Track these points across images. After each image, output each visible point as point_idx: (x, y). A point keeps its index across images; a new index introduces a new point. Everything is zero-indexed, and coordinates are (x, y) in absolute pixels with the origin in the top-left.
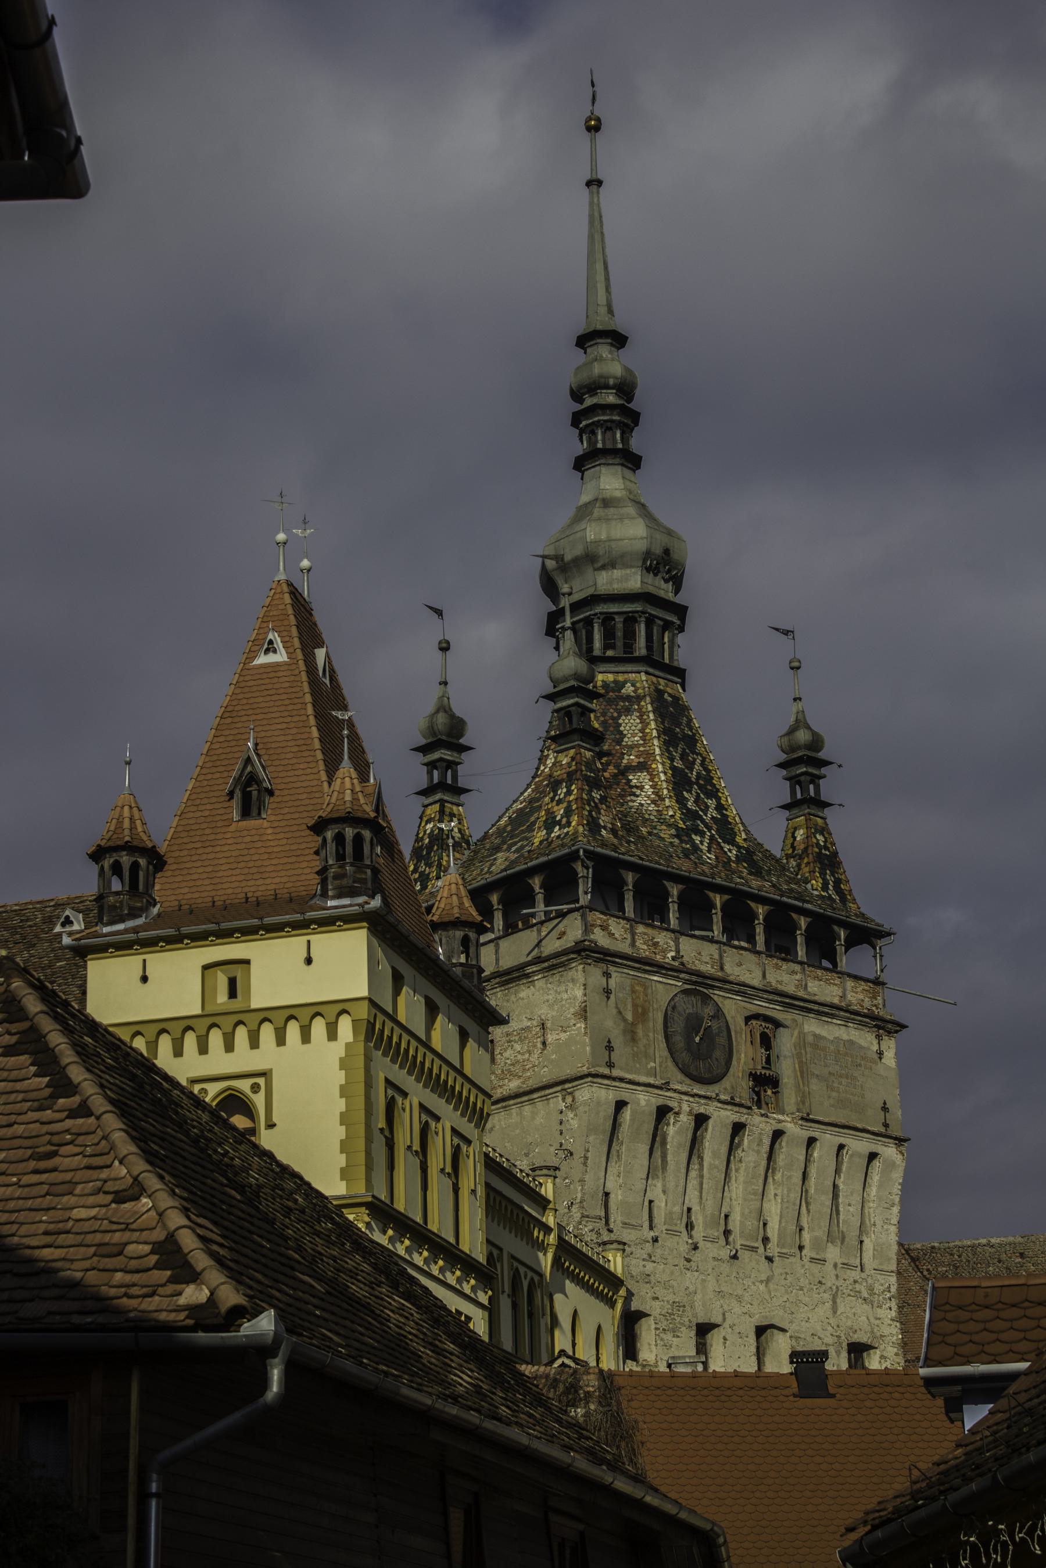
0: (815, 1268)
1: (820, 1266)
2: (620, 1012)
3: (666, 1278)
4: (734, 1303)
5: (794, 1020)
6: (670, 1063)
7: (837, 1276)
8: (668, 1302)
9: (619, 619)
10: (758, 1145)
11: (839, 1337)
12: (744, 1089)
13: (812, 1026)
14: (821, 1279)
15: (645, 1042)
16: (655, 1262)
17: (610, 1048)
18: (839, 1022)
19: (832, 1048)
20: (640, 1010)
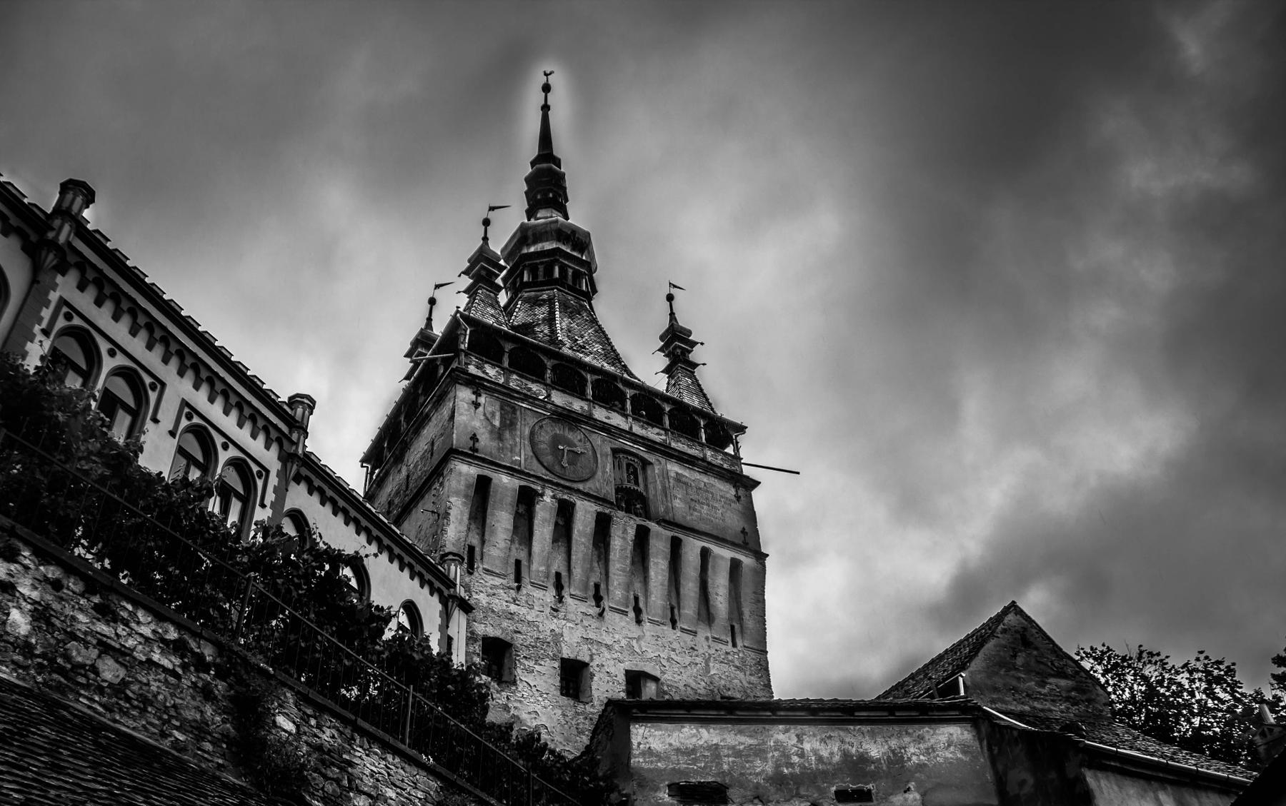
0: (688, 638)
1: (691, 636)
2: (488, 420)
3: (529, 618)
4: (603, 649)
5: (658, 460)
6: (535, 461)
7: (709, 647)
8: (531, 637)
9: (541, 268)
10: (623, 533)
11: (712, 691)
12: (612, 497)
13: (674, 468)
14: (693, 646)
15: (511, 443)
16: (518, 605)
17: (474, 438)
18: (701, 470)
19: (693, 485)
20: (508, 422)
